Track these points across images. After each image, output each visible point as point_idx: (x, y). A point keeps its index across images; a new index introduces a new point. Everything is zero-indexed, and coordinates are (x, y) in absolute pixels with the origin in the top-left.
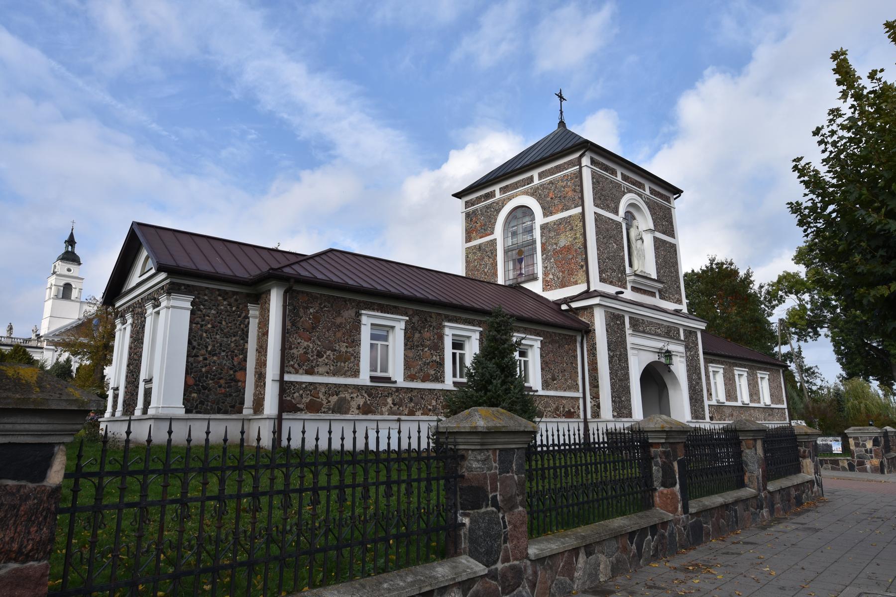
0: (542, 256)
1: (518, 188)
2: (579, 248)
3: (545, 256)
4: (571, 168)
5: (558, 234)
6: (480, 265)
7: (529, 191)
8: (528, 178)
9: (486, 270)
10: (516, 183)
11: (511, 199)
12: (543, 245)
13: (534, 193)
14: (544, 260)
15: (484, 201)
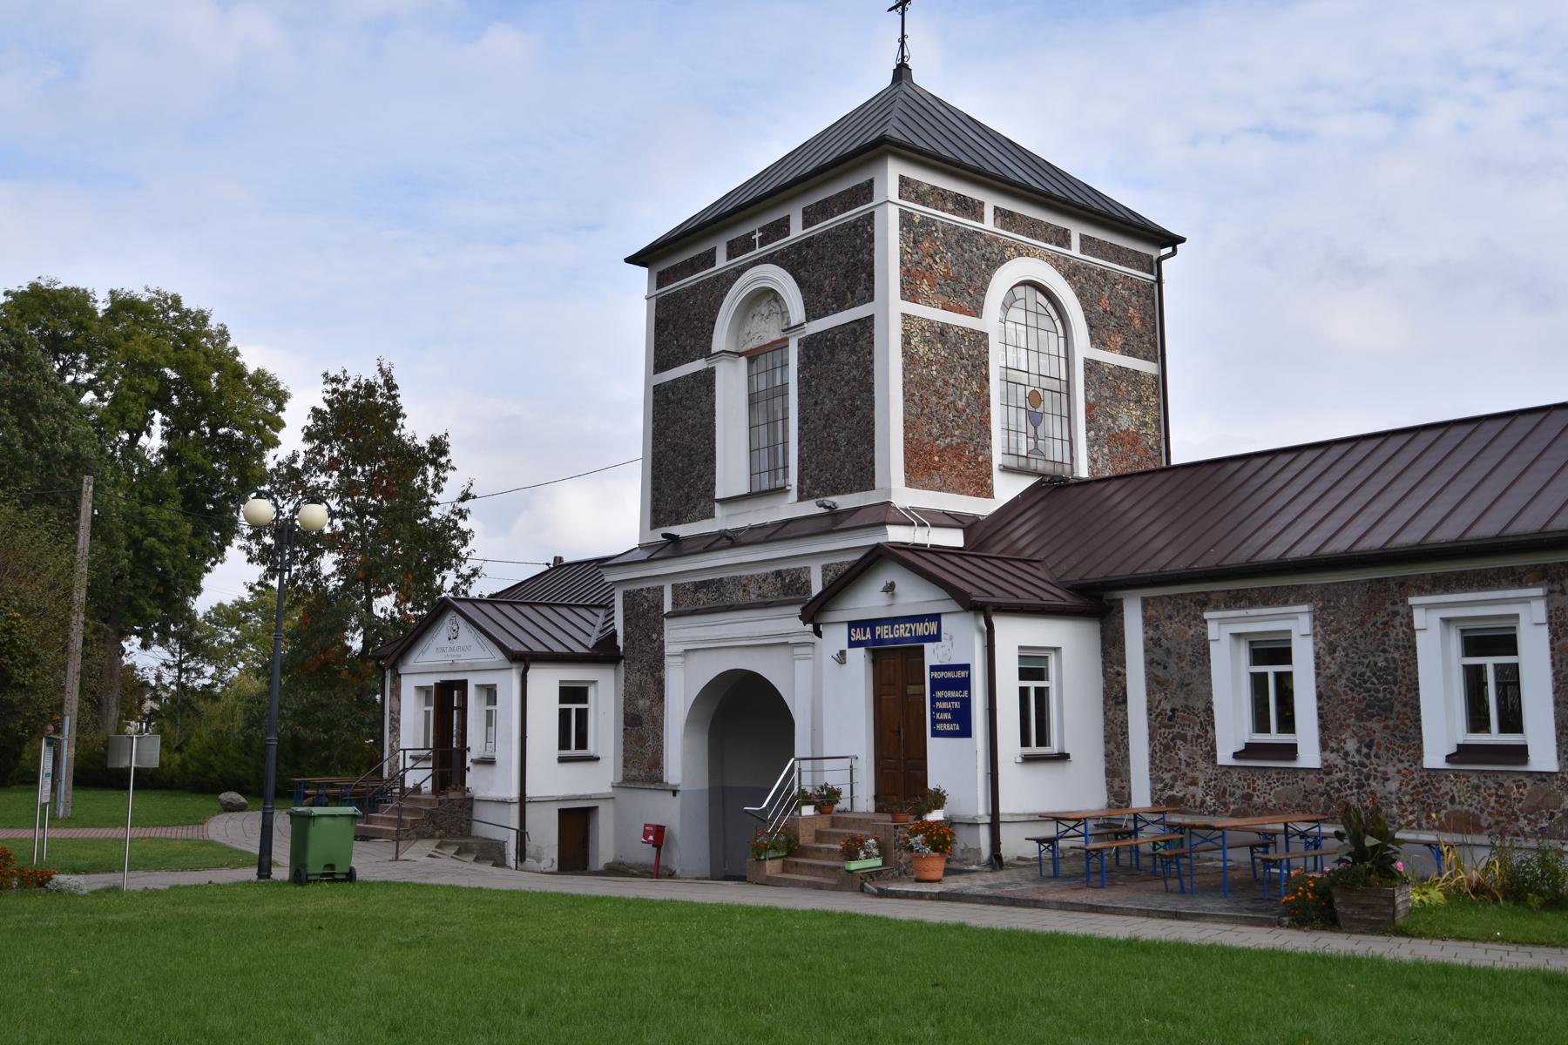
0: (1088, 431)
1: (1035, 237)
2: (1152, 449)
3: (1092, 433)
4: (1137, 269)
5: (1114, 397)
6: (946, 383)
7: (1061, 262)
8: (1057, 230)
9: (960, 404)
10: (1035, 223)
11: (1020, 255)
12: (1089, 408)
13: (1071, 272)
14: (1091, 443)
15: (953, 212)
